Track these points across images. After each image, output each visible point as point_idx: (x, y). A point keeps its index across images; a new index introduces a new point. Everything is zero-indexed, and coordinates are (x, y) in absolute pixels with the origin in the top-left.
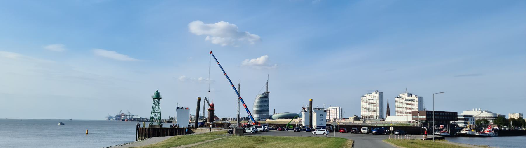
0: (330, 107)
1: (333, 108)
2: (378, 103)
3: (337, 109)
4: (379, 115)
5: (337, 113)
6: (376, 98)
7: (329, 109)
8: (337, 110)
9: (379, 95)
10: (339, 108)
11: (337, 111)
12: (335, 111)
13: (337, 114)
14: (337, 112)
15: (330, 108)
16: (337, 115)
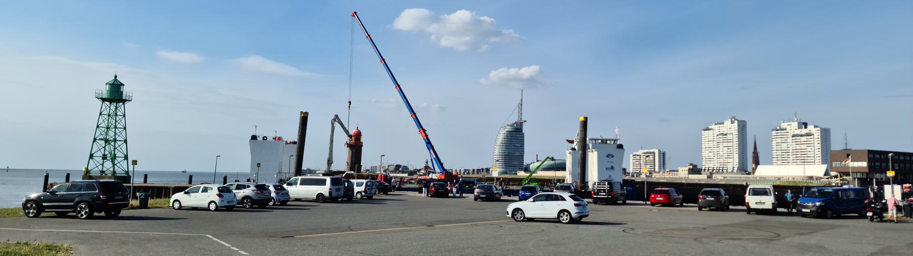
0: (642, 149)
1: (647, 151)
2: (737, 140)
3: (654, 153)
4: (738, 164)
5: (654, 161)
6: (733, 132)
7: (638, 153)
8: (654, 155)
9: (739, 126)
10: (660, 151)
11: (654, 157)
12: (651, 158)
13: (654, 163)
14: (654, 159)
15: (640, 151)
16: (654, 165)
